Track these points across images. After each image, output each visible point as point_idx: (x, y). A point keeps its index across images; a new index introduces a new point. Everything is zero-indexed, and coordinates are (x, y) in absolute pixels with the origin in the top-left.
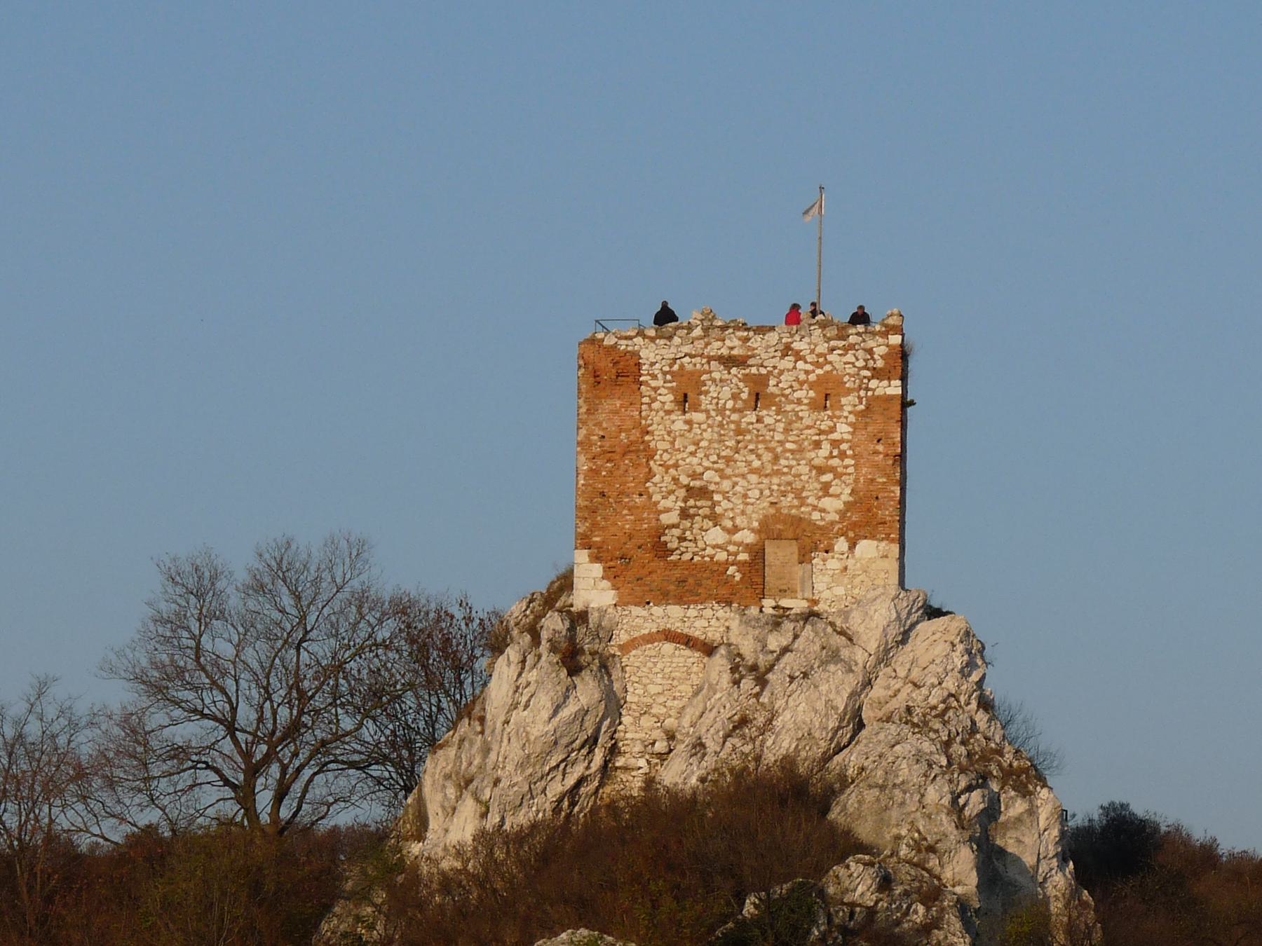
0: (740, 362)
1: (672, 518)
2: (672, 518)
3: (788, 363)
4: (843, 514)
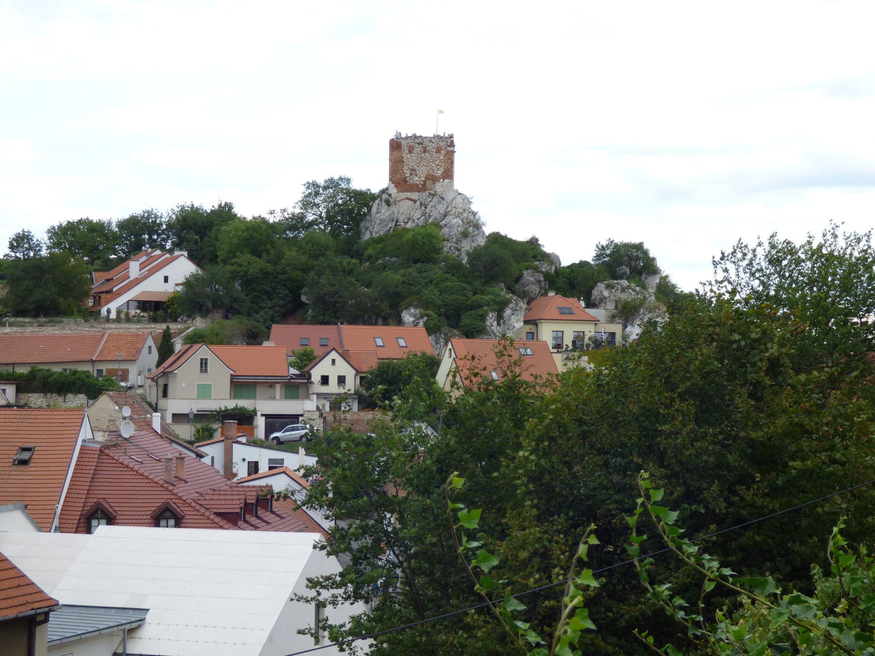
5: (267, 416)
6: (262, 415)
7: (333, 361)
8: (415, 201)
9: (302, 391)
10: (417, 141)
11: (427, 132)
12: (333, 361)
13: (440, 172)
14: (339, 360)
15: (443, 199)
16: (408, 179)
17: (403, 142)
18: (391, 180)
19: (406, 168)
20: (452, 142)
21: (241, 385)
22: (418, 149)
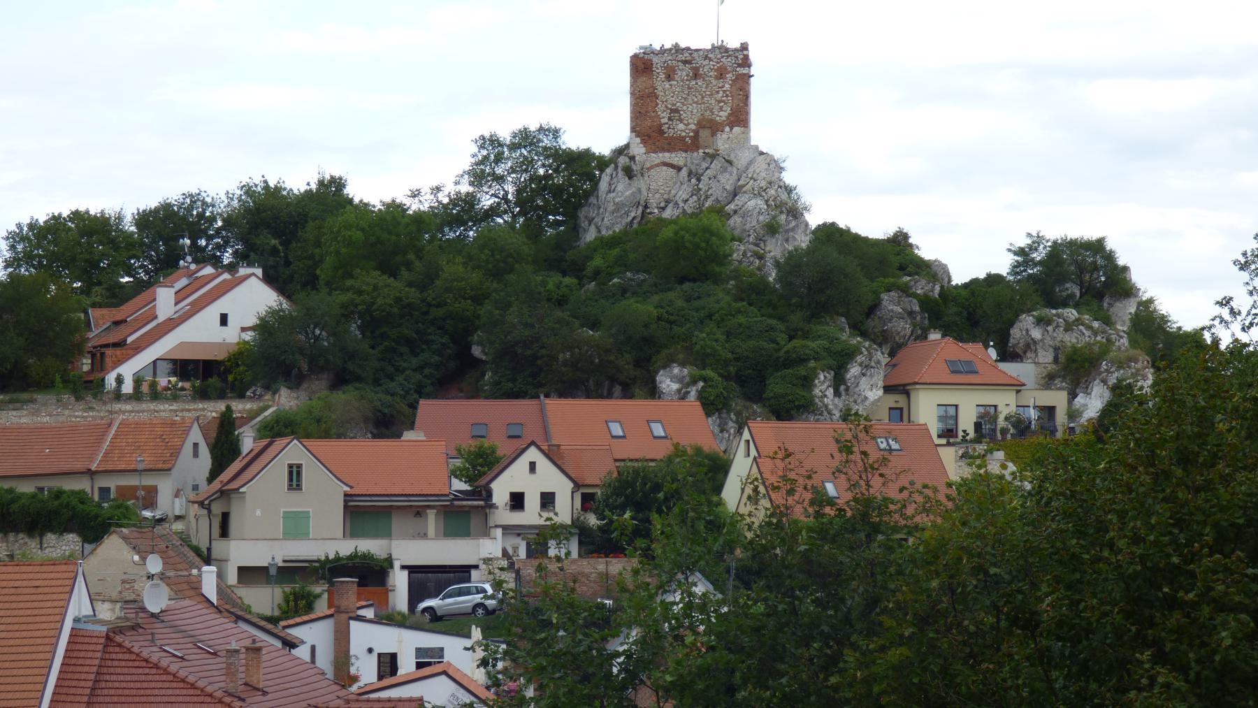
0: (689, 62)
1: (666, 120)
2: (666, 120)
3: (707, 62)
4: (728, 117)
5: (412, 569)
6: (403, 567)
7: (533, 467)
8: (679, 169)
9: (475, 522)
10: (680, 57)
11: (699, 39)
12: (533, 467)
14: (543, 464)
15: (730, 162)
16: (665, 127)
17: (655, 60)
18: (633, 130)
19: (660, 107)
20: (746, 58)
21: (363, 513)
22: (683, 72)
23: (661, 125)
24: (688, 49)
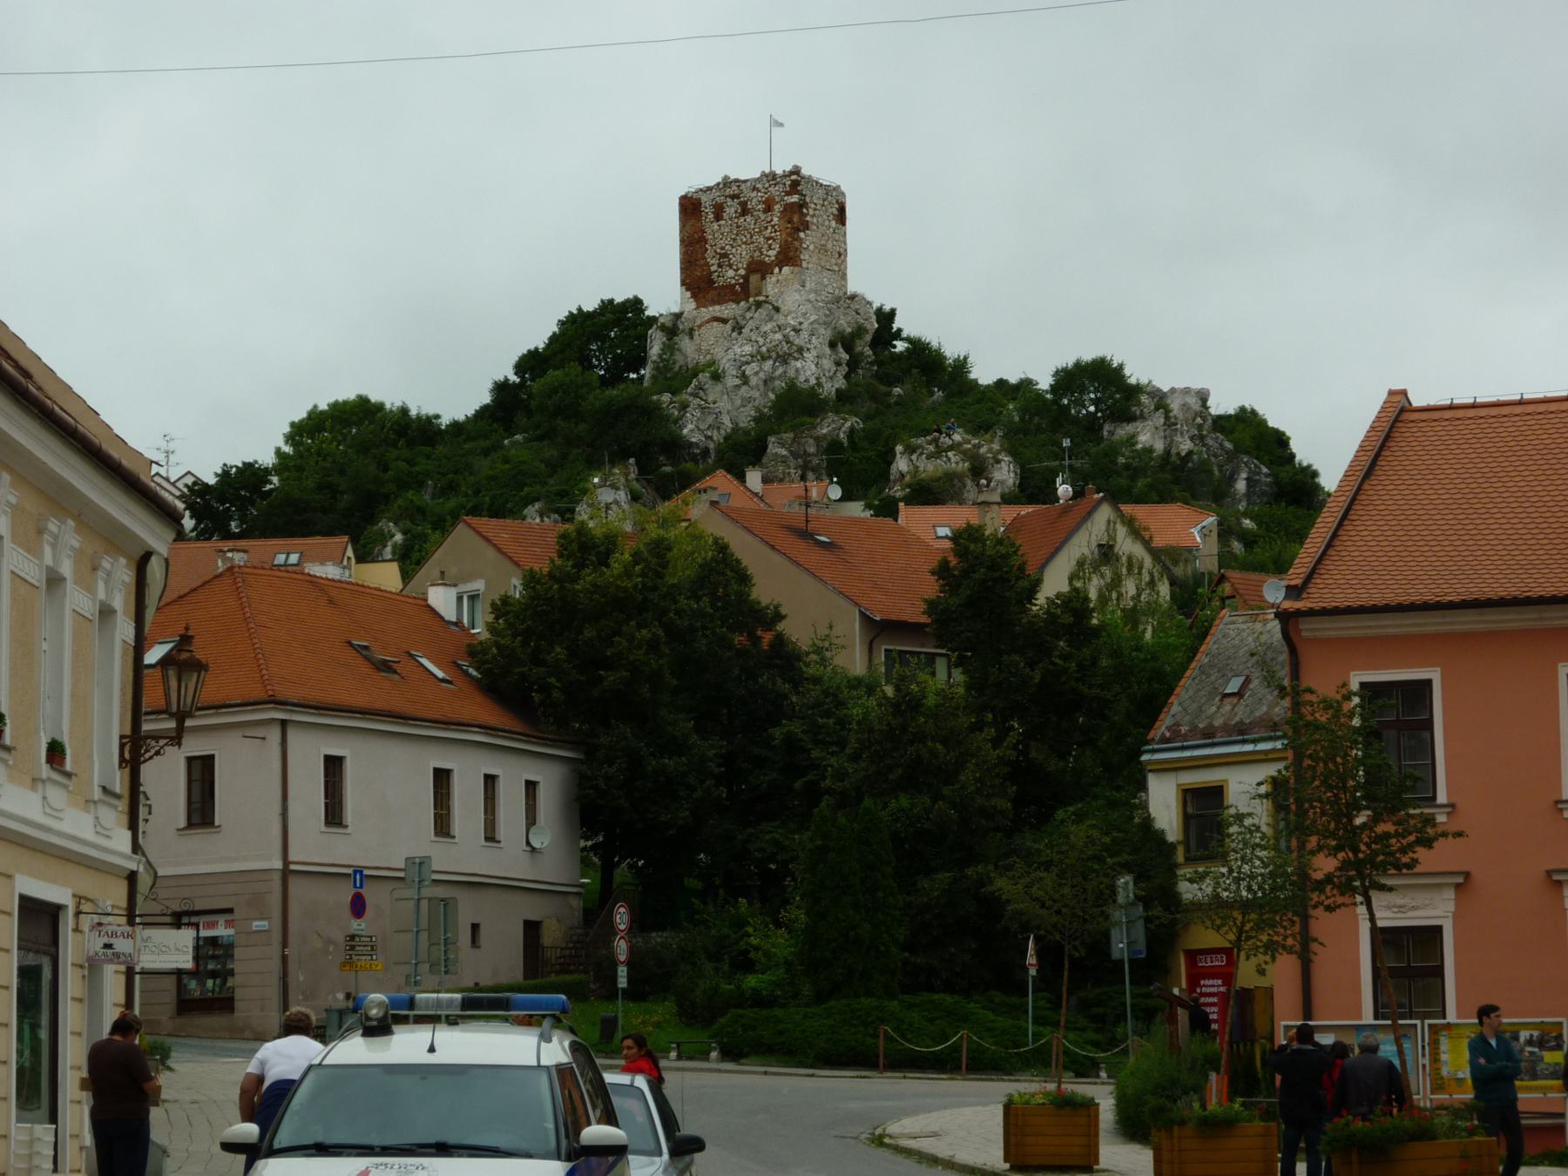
13: (772, 253)
15: (777, 310)
17: (704, 198)
19: (710, 253)
22: (731, 209)
23: (711, 273)
24: (737, 181)
